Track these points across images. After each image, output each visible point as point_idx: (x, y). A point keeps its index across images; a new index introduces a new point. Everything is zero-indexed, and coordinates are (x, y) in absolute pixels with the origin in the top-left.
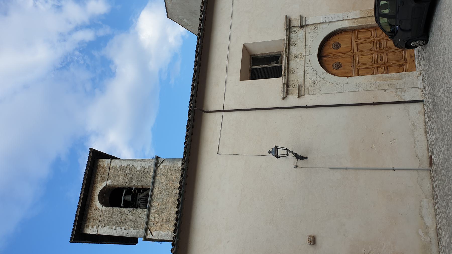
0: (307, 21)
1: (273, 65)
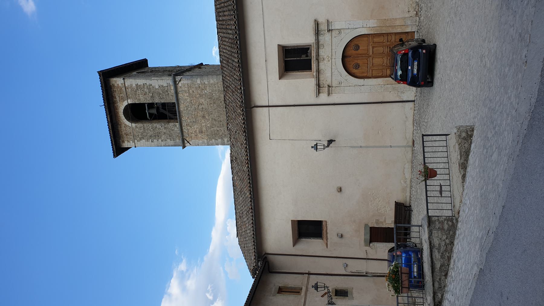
0: (332, 26)
1: (304, 57)
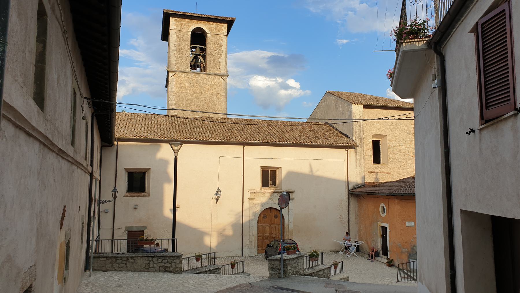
1: (270, 182)
